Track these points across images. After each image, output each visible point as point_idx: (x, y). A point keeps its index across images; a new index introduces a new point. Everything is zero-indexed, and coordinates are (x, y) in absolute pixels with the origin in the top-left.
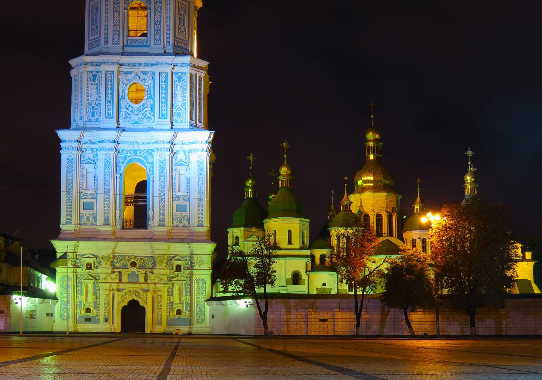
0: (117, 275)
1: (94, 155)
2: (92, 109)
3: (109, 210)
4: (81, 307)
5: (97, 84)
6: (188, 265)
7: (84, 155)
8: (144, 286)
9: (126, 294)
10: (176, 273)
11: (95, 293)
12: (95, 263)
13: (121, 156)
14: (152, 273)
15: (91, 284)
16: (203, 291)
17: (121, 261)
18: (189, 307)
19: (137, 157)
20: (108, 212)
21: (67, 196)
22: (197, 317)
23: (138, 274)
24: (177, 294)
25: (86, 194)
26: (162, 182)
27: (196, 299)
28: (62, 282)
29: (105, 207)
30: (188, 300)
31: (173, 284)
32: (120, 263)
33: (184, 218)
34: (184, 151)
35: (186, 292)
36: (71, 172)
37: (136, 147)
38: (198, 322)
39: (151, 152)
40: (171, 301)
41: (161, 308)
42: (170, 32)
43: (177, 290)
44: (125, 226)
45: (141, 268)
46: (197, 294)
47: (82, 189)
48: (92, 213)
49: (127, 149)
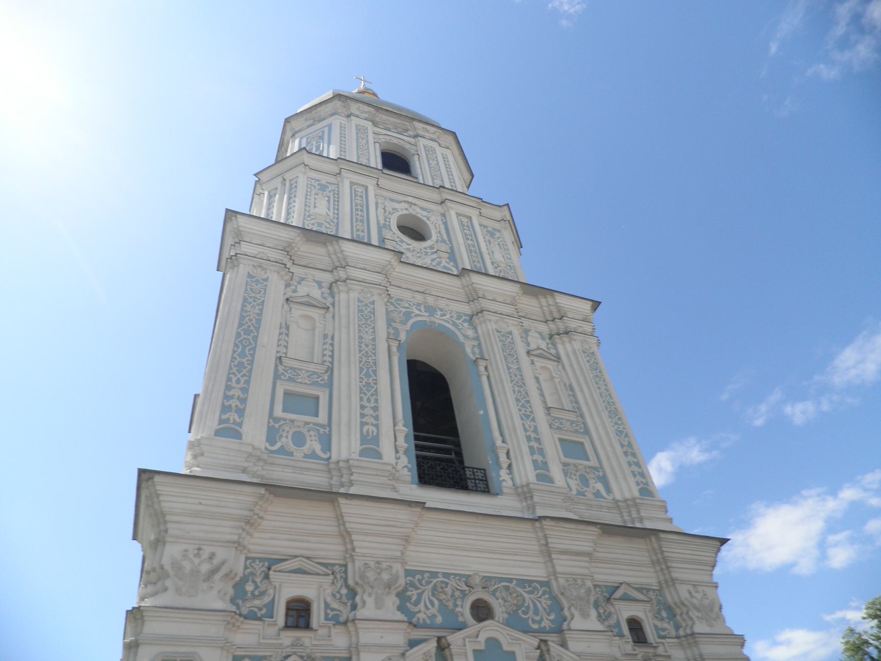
1: (323, 293)
3: (377, 418)
6: (662, 619)
7: (296, 286)
12: (329, 599)
13: (397, 311)
14: (564, 644)
17: (433, 595)
19: (437, 321)
20: (374, 422)
21: (233, 358)
25: (296, 372)
26: (516, 376)
29: (362, 407)
34: (540, 333)
36: (258, 305)
37: (431, 300)
39: (467, 318)
47: (284, 355)
48: (314, 424)
49: (411, 302)
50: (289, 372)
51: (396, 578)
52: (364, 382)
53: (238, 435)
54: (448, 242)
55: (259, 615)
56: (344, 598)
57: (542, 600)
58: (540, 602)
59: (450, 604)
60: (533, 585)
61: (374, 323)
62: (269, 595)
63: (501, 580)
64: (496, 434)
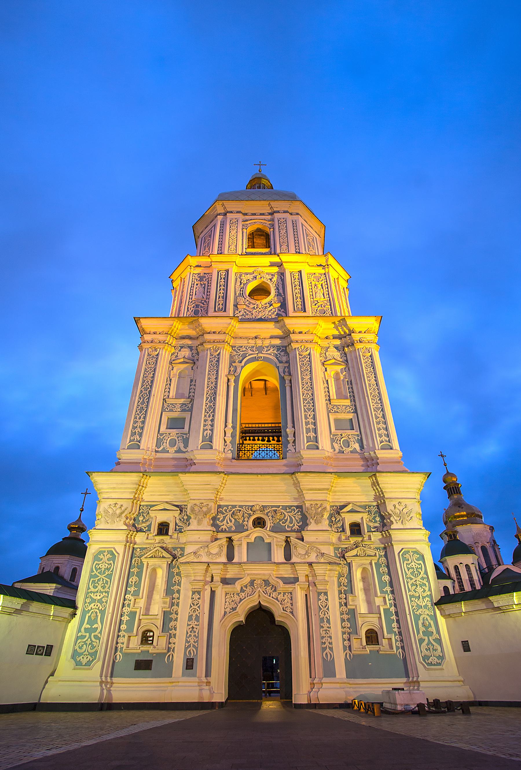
0: (221, 547)
1: (192, 354)
2: (195, 307)
4: (130, 629)
5: (205, 284)
6: (376, 522)
8: (286, 571)
9: (242, 590)
10: (353, 540)
11: (169, 592)
12: (177, 521)
15: (161, 568)
16: (423, 578)
17: (232, 517)
18: (395, 623)
22: (423, 650)
23: (270, 544)
24: (361, 590)
27: (412, 601)
28: (96, 562)
30: (391, 605)
31: (349, 565)
32: (231, 521)
33: (352, 440)
35: (382, 584)
37: (259, 342)
38: (428, 664)
39: (284, 348)
40: (348, 607)
41: (328, 625)
42: (299, 245)
43: (358, 580)
44: (241, 456)
45: (276, 529)
46: (410, 587)
48: (181, 434)
50: (170, 406)
51: (209, 510)
52: (208, 406)
53: (138, 447)
54: (282, 294)
55: (145, 530)
56: (185, 520)
57: (296, 516)
58: (295, 517)
59: (241, 521)
60: (292, 508)
61: (218, 368)
62: (150, 521)
63: (273, 506)
64: (290, 424)
